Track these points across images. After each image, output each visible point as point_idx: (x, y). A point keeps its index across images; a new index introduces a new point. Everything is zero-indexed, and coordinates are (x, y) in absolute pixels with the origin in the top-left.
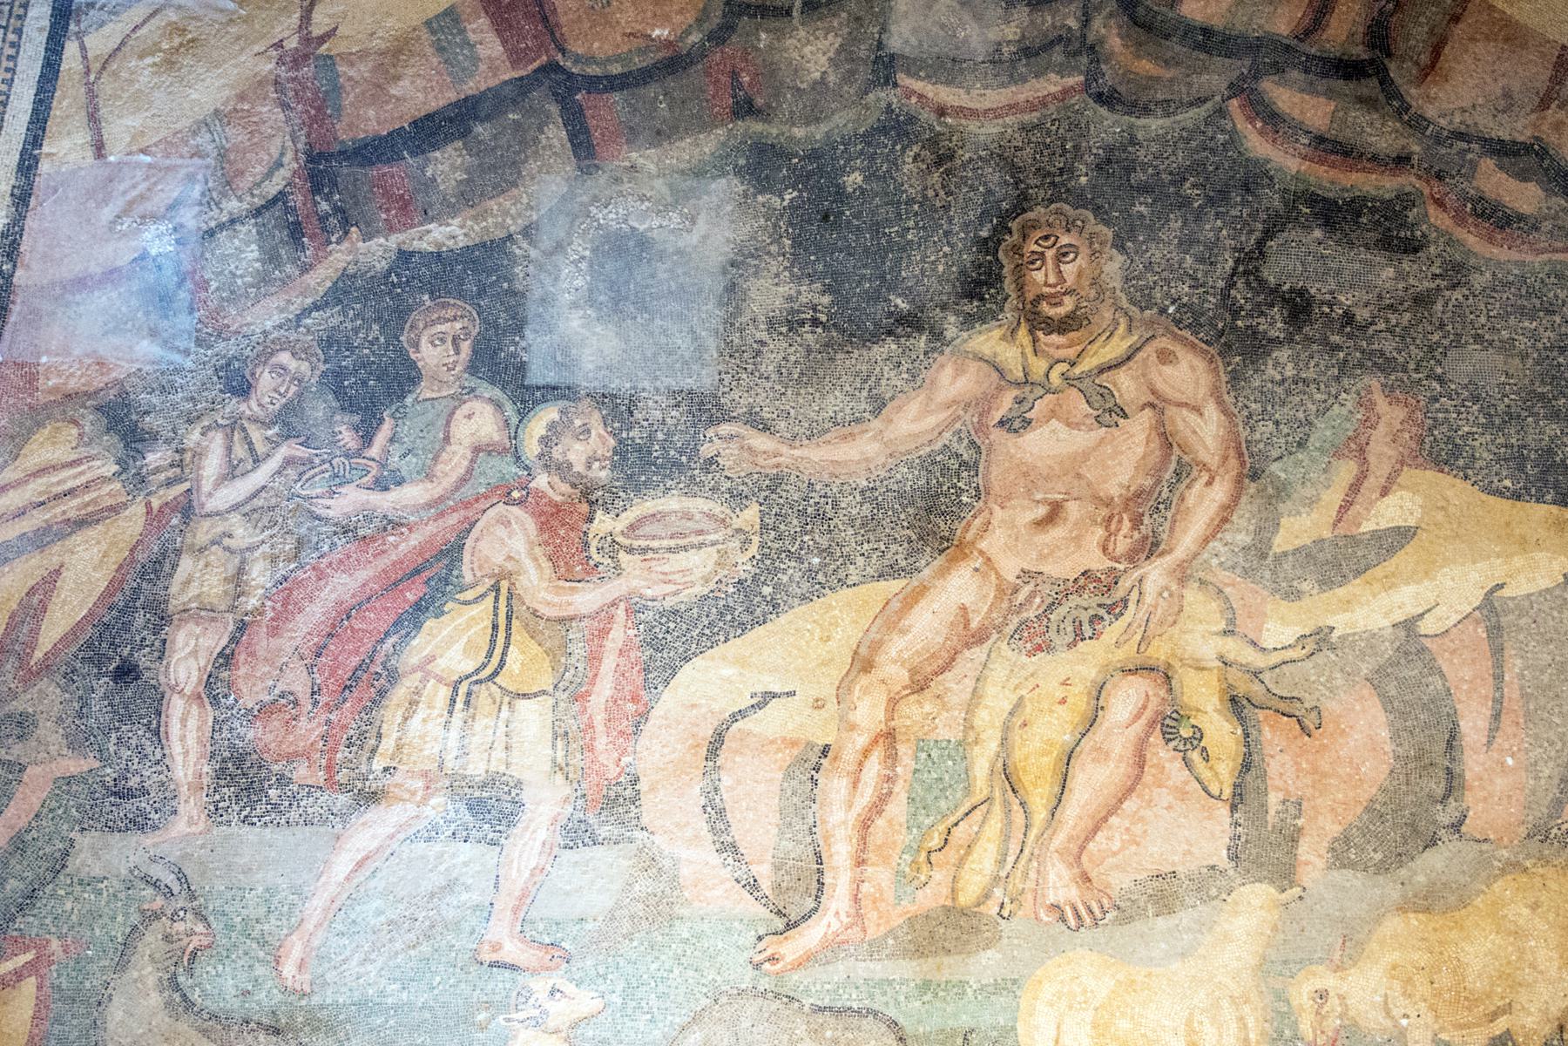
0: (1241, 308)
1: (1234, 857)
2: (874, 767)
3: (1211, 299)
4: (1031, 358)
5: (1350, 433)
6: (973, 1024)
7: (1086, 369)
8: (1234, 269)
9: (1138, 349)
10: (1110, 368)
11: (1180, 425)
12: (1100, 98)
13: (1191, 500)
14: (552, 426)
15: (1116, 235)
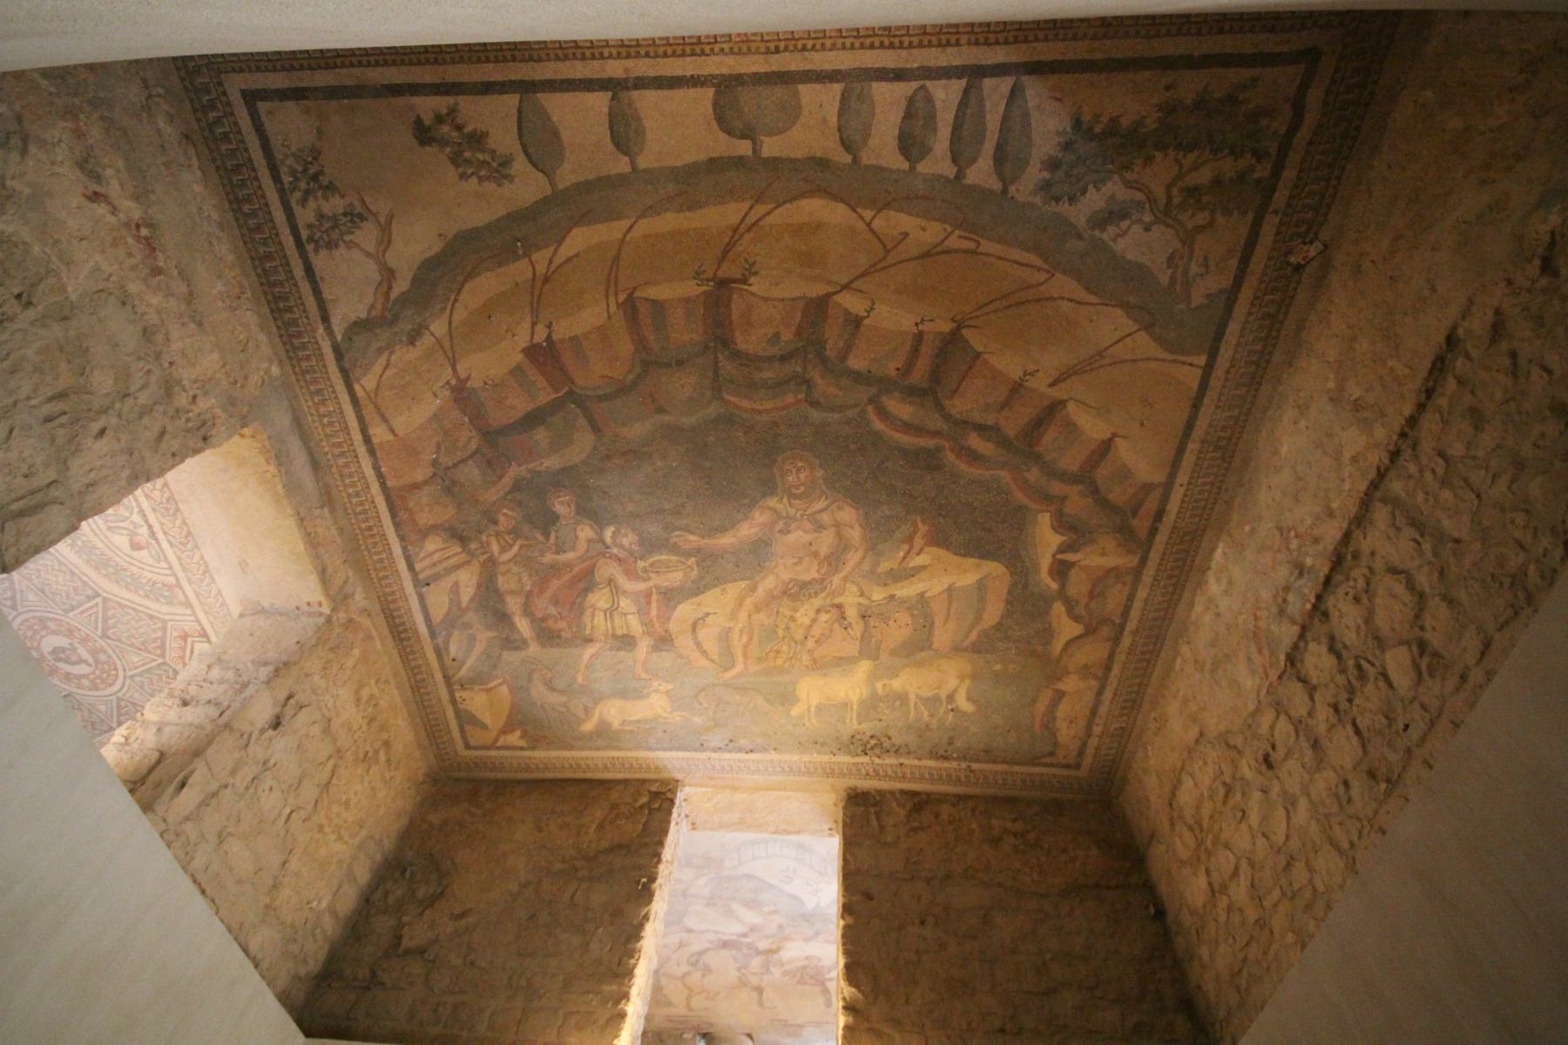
1: (860, 653)
8: (867, 478)
12: (812, 404)
13: (850, 555)
14: (614, 532)
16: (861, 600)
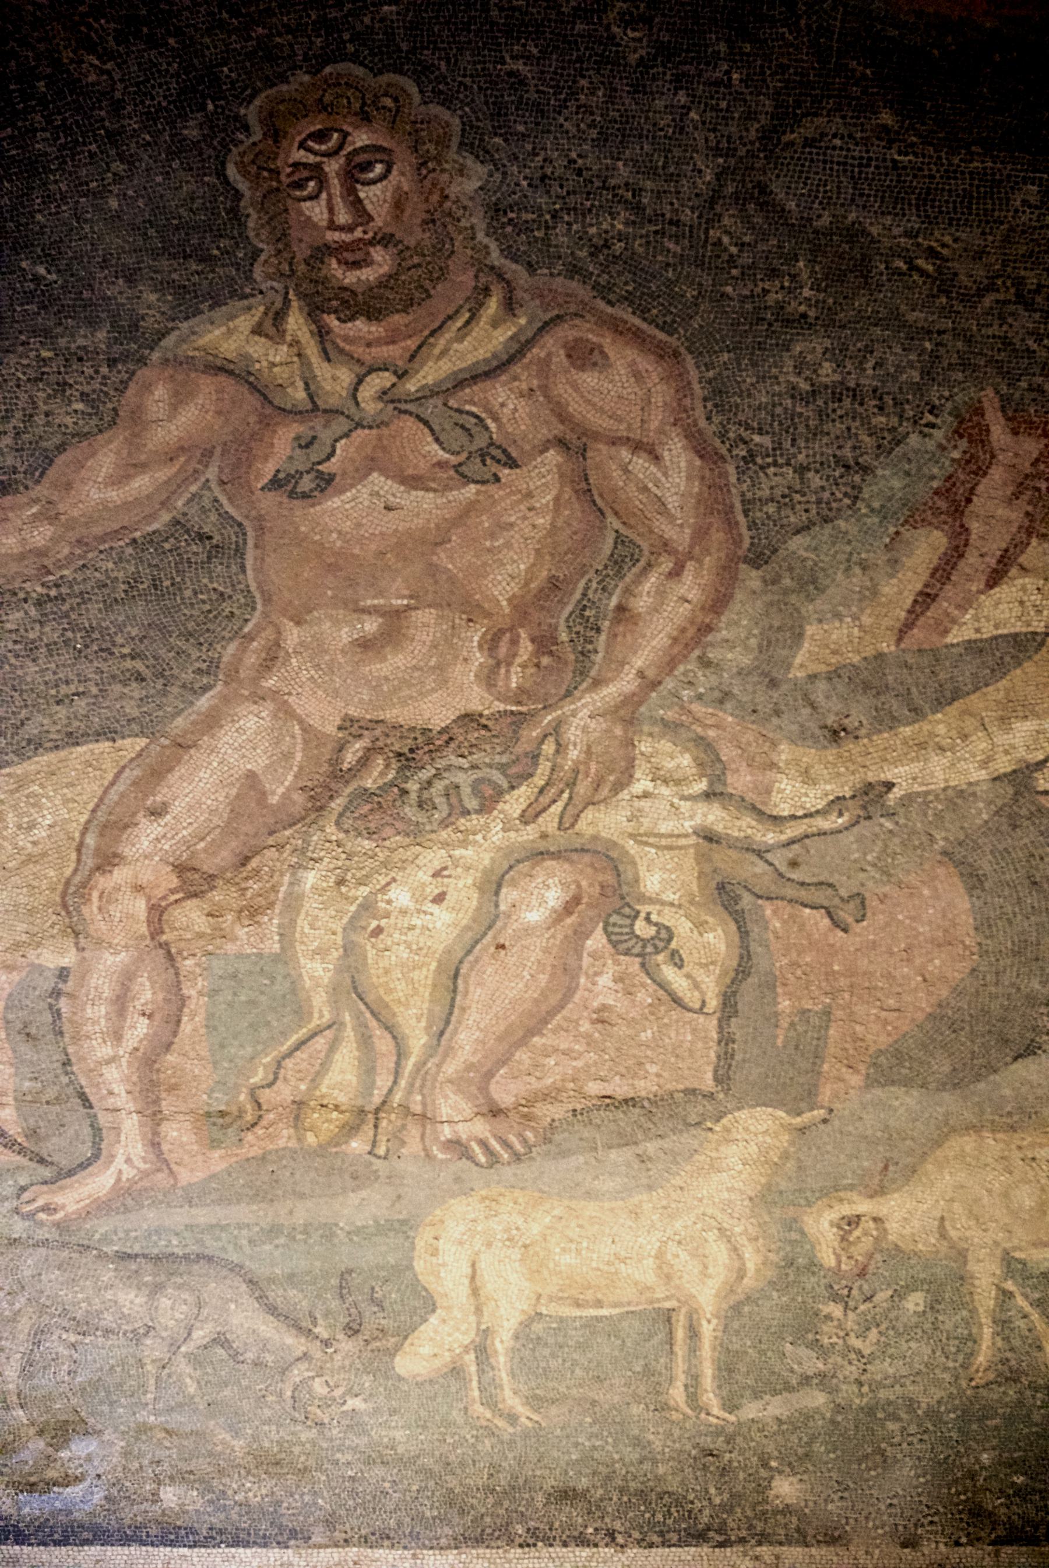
0: (732, 260)
2: (145, 993)
3: (671, 246)
4: (322, 370)
5: (935, 484)
6: (351, 1265)
7: (430, 380)
9: (529, 343)
10: (475, 378)
11: (617, 475)
15: (467, 126)
16: (714, 816)
